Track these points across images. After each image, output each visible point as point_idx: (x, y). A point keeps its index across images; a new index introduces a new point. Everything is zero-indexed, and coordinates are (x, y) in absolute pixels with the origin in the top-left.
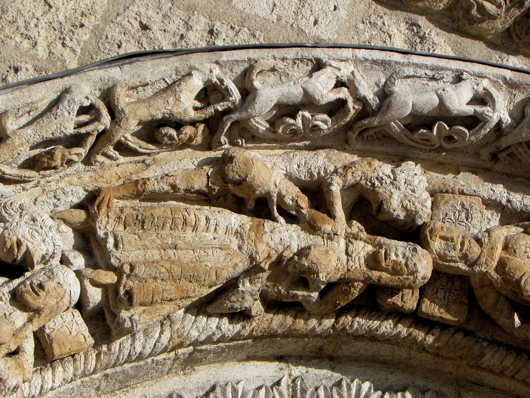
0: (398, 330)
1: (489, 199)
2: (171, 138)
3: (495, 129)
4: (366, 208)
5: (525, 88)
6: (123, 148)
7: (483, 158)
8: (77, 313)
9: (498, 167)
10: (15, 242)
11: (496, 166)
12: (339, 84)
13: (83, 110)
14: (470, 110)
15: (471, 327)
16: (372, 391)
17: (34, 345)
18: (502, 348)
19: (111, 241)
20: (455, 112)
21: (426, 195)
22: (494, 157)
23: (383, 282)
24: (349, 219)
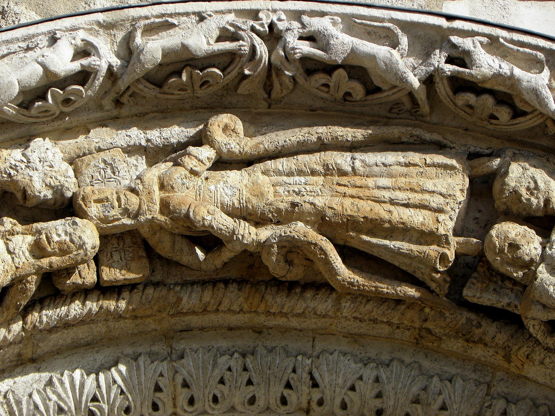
0: (88, 308)
1: (129, 146)
3: (108, 76)
5: (121, 25)
7: (107, 108)
9: (125, 111)
11: (123, 111)
14: (76, 66)
15: (158, 277)
16: (85, 377)
18: (195, 286)
20: (63, 74)
21: (65, 165)
22: (118, 103)
23: (55, 266)
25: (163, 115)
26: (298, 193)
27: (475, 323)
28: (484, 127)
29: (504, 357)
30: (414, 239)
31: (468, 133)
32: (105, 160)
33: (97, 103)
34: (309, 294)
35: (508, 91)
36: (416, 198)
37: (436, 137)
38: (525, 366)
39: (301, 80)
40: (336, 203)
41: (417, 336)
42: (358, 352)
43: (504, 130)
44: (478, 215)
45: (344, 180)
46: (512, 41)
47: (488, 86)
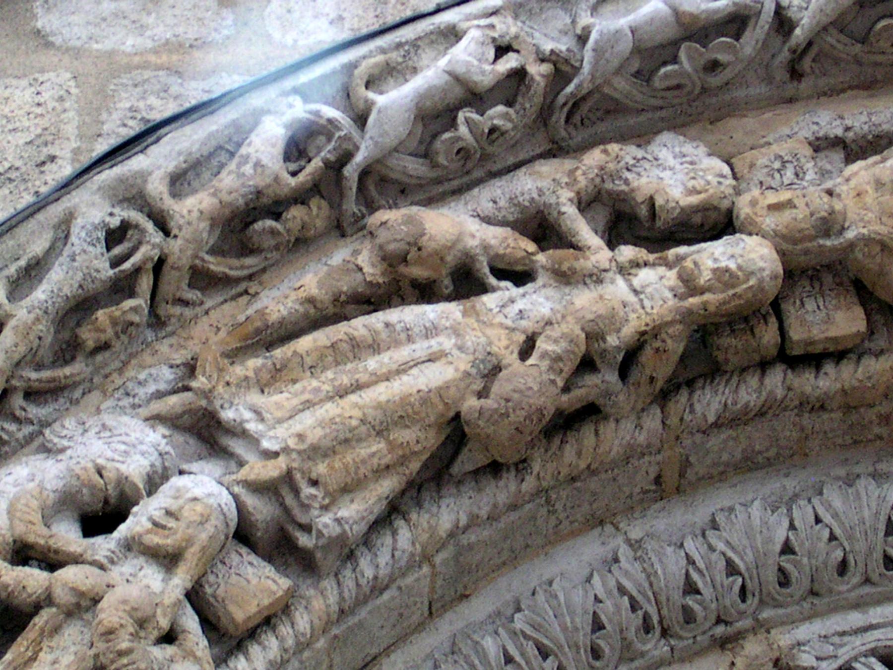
0: (769, 388)
1: (818, 139)
2: (273, 232)
3: (776, 26)
4: (631, 223)
6: (203, 279)
8: (244, 550)
9: (805, 86)
10: (93, 470)
11: (803, 85)
12: (502, 50)
13: (115, 236)
17: (196, 618)
19: (248, 415)
20: (703, 16)
22: (795, 74)
23: (712, 309)
24: (612, 245)
32: (781, 157)
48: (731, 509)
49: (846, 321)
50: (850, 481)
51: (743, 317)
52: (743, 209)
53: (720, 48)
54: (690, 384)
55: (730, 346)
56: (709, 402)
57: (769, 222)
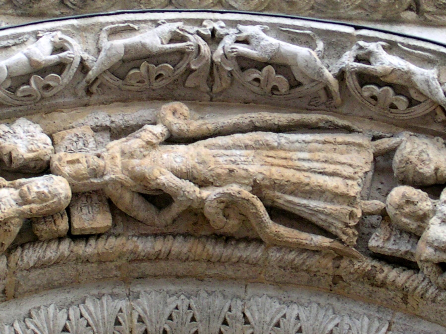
0: (61, 251)
1: (97, 126)
3: (80, 69)
5: (92, 29)
7: (80, 94)
9: (94, 98)
14: (55, 57)
16: (58, 311)
18: (149, 237)
20: (43, 63)
22: (89, 92)
23: (34, 212)
25: (126, 100)
26: (234, 162)
27: (378, 268)
28: (386, 116)
29: (402, 299)
30: (329, 199)
31: (373, 121)
32: (77, 135)
33: (71, 88)
34: (242, 246)
35: (405, 84)
36: (330, 168)
37: (346, 123)
38: (420, 306)
39: (237, 75)
40: (265, 170)
41: (331, 283)
42: (283, 296)
43: (401, 118)
44: (380, 186)
45: (271, 153)
46: (409, 46)
47: (388, 80)
48: (39, 308)
49: (102, 220)
50: (100, 297)
51: (49, 216)
52: (55, 163)
53: (51, 78)
54: (22, 246)
55: (42, 228)
56: (31, 255)
57: (67, 169)
